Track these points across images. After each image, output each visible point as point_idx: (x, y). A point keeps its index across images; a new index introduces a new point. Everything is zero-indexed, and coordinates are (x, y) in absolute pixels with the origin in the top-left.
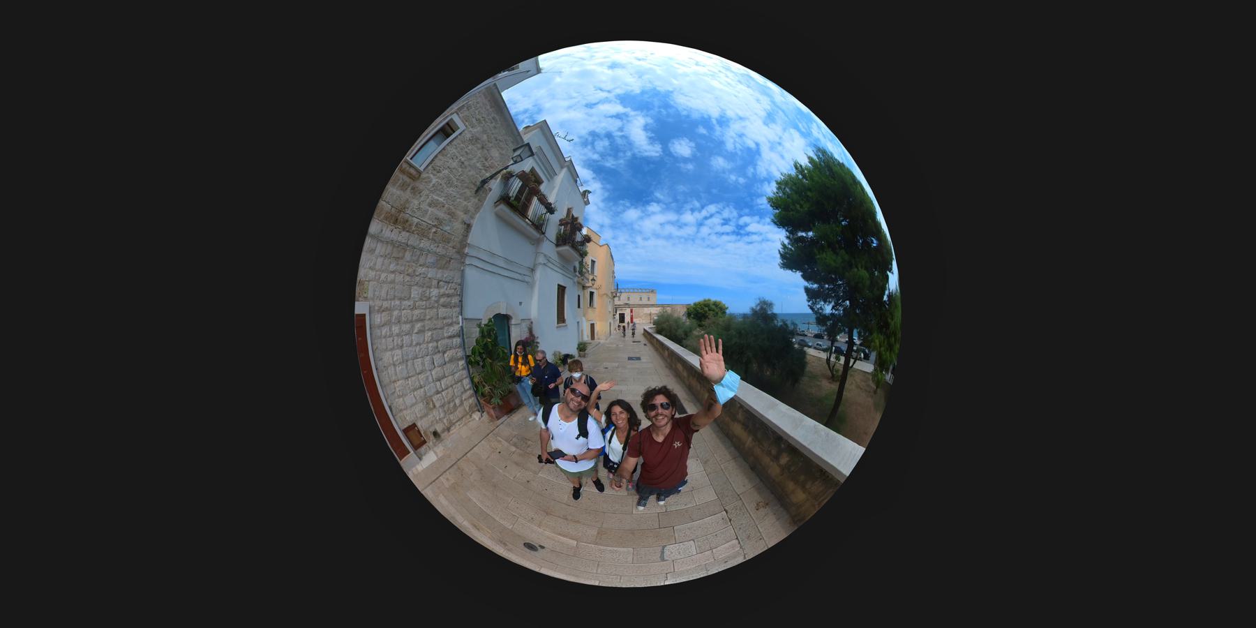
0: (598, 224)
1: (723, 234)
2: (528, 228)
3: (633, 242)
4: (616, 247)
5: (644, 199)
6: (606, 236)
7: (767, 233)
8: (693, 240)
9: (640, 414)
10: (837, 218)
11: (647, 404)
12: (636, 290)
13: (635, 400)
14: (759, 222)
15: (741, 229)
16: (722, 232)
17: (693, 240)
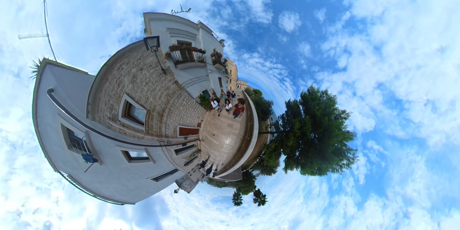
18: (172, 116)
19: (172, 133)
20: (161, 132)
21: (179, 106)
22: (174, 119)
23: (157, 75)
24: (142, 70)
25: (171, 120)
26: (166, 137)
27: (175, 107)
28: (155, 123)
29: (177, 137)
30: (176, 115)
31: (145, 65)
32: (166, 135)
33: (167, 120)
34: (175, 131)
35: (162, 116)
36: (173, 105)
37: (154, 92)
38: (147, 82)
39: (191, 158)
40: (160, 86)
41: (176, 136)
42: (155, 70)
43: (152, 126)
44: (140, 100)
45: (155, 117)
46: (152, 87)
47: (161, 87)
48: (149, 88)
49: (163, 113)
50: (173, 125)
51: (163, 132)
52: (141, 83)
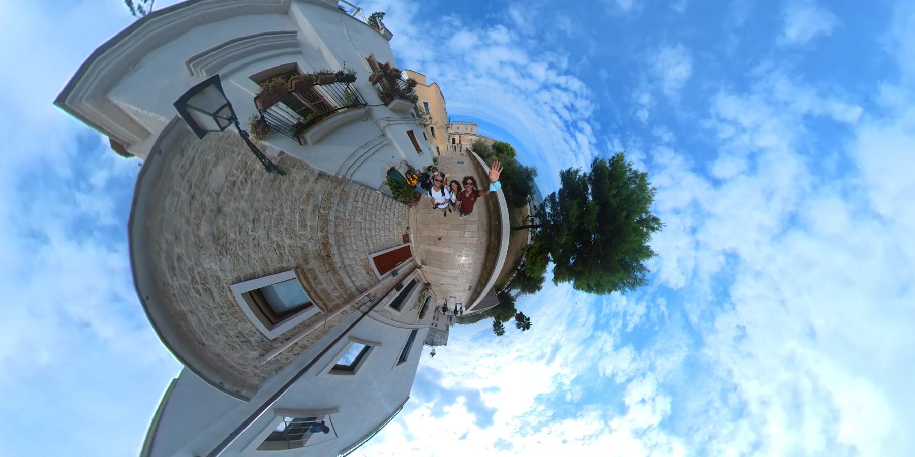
0: (418, 61)
1: (557, 113)
2: (349, 114)
3: (462, 79)
4: (445, 85)
5: (487, 16)
6: (432, 73)
7: (583, 154)
8: (527, 97)
9: (462, 186)
10: (598, 232)
11: (465, 183)
12: (463, 123)
13: (460, 181)
14: (590, 143)
15: (573, 126)
16: (558, 111)
17: (527, 97)
18: (348, 244)
19: (367, 279)
20: (347, 291)
21: (352, 217)
22: (355, 247)
23: (266, 189)
24: (219, 210)
25: (349, 253)
26: (361, 293)
27: (346, 223)
28: (325, 282)
29: (379, 281)
30: (354, 236)
31: (218, 195)
32: (359, 288)
33: (342, 259)
34: (369, 271)
35: (329, 256)
36: (338, 220)
37: (282, 224)
38: (251, 218)
39: (422, 302)
40: (289, 203)
41: (376, 280)
42: (252, 183)
43: (324, 291)
44: (267, 264)
45: (317, 270)
46: (271, 217)
47: (292, 202)
48: (267, 225)
49: (327, 251)
50: (358, 261)
51: (350, 286)
52: (240, 233)
